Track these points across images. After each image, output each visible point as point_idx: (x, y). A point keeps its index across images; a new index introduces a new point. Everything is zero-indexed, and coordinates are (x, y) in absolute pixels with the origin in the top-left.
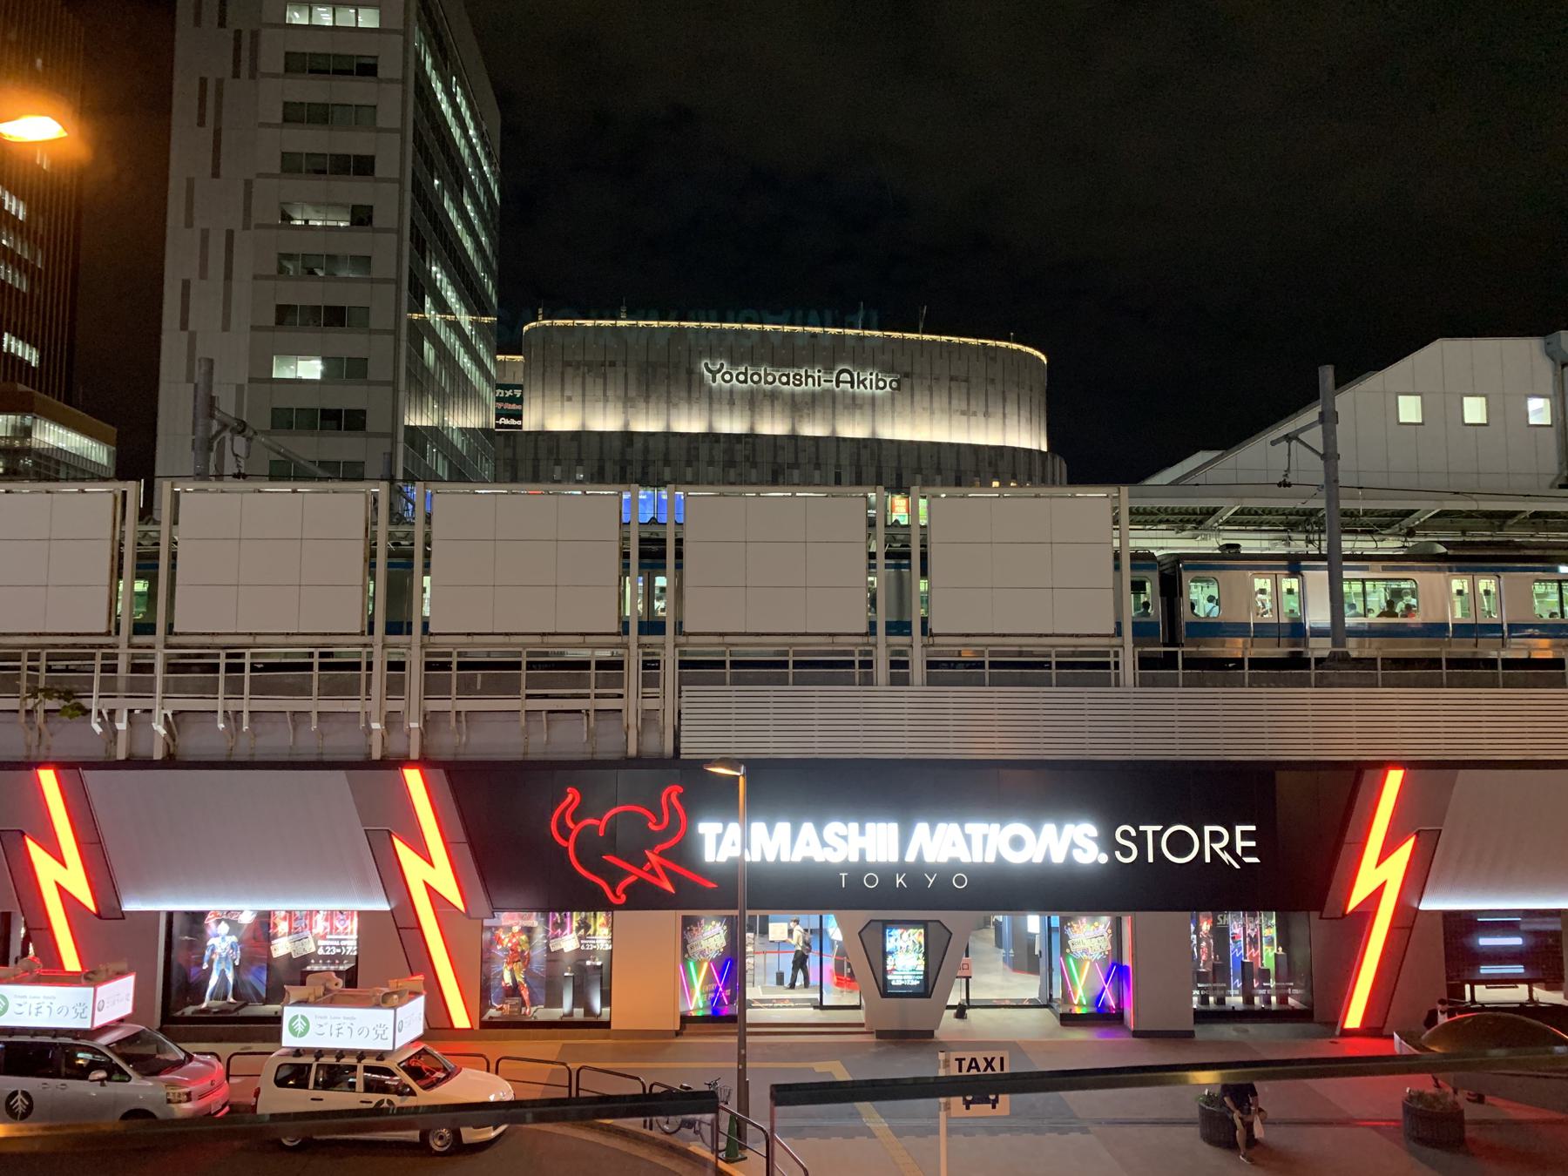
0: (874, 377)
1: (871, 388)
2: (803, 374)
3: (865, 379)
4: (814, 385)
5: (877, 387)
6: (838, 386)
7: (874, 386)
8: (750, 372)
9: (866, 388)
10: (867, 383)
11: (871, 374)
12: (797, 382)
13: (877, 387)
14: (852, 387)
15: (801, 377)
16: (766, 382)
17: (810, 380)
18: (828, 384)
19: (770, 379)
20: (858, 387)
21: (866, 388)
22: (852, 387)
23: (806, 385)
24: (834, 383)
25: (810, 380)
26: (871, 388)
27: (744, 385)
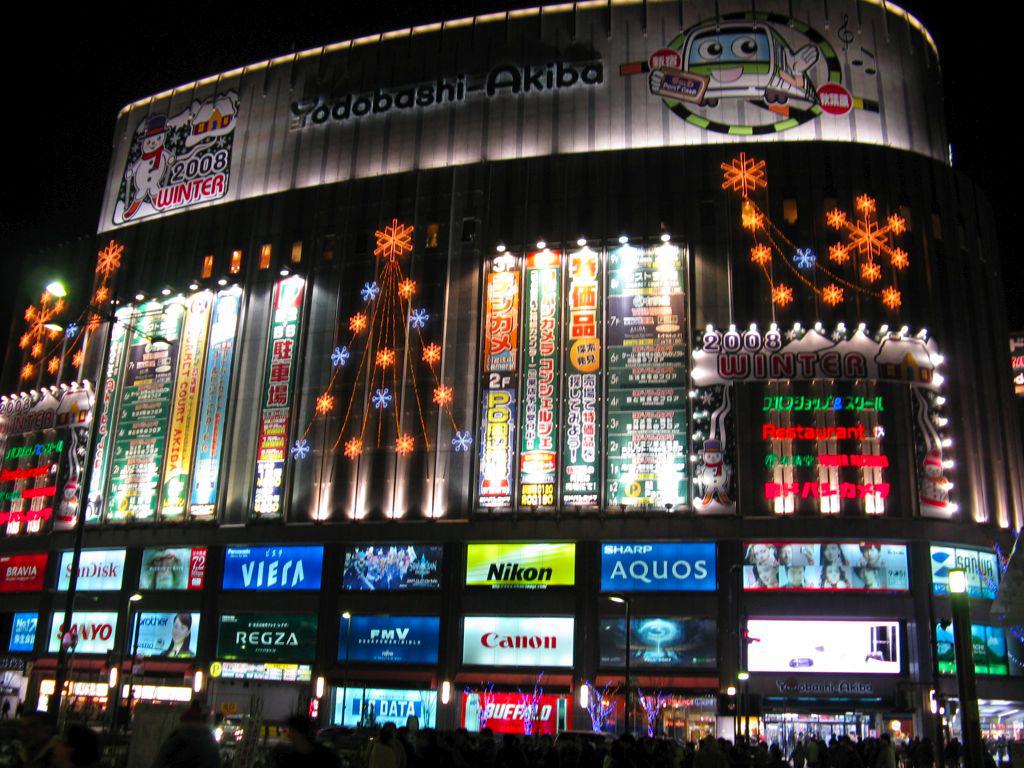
0: (554, 70)
1: (550, 85)
2: (435, 88)
3: (540, 74)
4: (451, 97)
5: (561, 83)
6: (491, 92)
7: (555, 83)
8: (353, 102)
9: (539, 87)
10: (543, 79)
11: (550, 65)
12: (427, 92)
13: (561, 83)
14: (516, 89)
15: (432, 90)
16: (377, 109)
17: (445, 94)
18: (476, 93)
19: (382, 103)
20: (527, 88)
21: (539, 87)
22: (516, 89)
23: (439, 99)
24: (485, 91)
25: (445, 94)
26: (550, 85)
27: (344, 120)
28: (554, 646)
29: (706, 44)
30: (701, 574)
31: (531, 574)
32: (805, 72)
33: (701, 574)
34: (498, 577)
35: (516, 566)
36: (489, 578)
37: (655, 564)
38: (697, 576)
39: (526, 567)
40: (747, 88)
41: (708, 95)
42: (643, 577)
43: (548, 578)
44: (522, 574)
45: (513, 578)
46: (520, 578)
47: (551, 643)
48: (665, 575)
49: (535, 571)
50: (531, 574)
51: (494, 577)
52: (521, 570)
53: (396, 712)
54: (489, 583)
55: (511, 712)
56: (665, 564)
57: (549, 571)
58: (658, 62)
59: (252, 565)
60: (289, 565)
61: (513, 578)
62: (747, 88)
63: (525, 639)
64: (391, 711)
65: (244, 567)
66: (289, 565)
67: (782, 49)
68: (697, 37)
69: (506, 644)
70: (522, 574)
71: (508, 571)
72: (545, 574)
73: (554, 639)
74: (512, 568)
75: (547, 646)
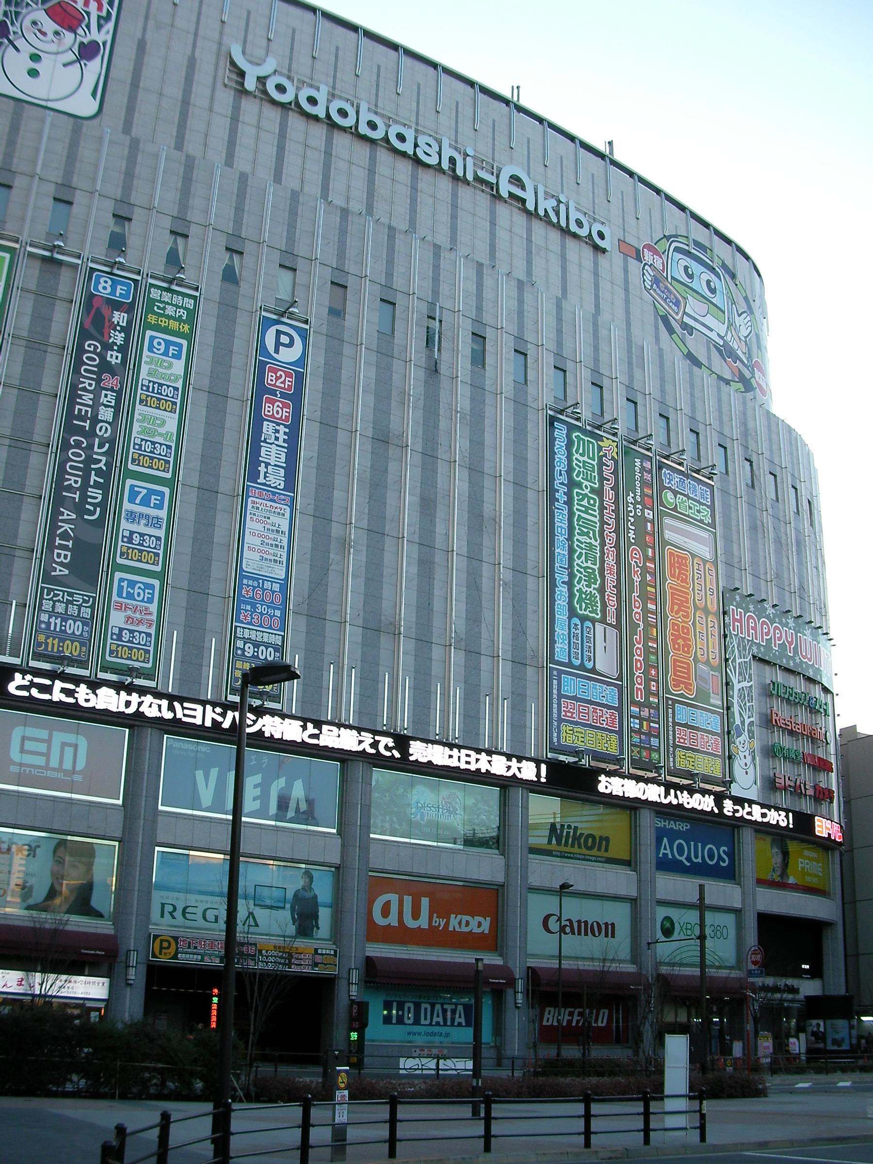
28: (613, 936)
29: (685, 261)
30: (724, 861)
31: (590, 840)
32: (746, 337)
33: (724, 861)
34: (559, 842)
35: (576, 828)
36: (550, 842)
37: (692, 843)
38: (721, 863)
39: (586, 832)
40: (711, 330)
41: (686, 319)
42: (683, 859)
43: (606, 850)
44: (582, 841)
45: (573, 846)
46: (580, 847)
47: (609, 930)
48: (699, 860)
49: (593, 837)
50: (590, 840)
51: (554, 841)
52: (582, 834)
53: (441, 1020)
54: (549, 847)
55: (570, 1018)
56: (700, 845)
57: (607, 839)
58: (648, 256)
59: (214, 772)
60: (281, 782)
61: (573, 846)
62: (711, 330)
63: (586, 922)
64: (435, 1019)
65: (199, 774)
66: (281, 782)
67: (732, 304)
68: (677, 249)
69: (568, 930)
70: (582, 841)
71: (568, 833)
72: (604, 843)
73: (613, 925)
74: (572, 831)
75: (606, 936)
